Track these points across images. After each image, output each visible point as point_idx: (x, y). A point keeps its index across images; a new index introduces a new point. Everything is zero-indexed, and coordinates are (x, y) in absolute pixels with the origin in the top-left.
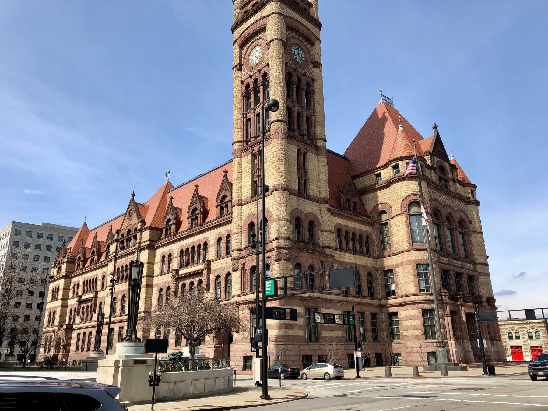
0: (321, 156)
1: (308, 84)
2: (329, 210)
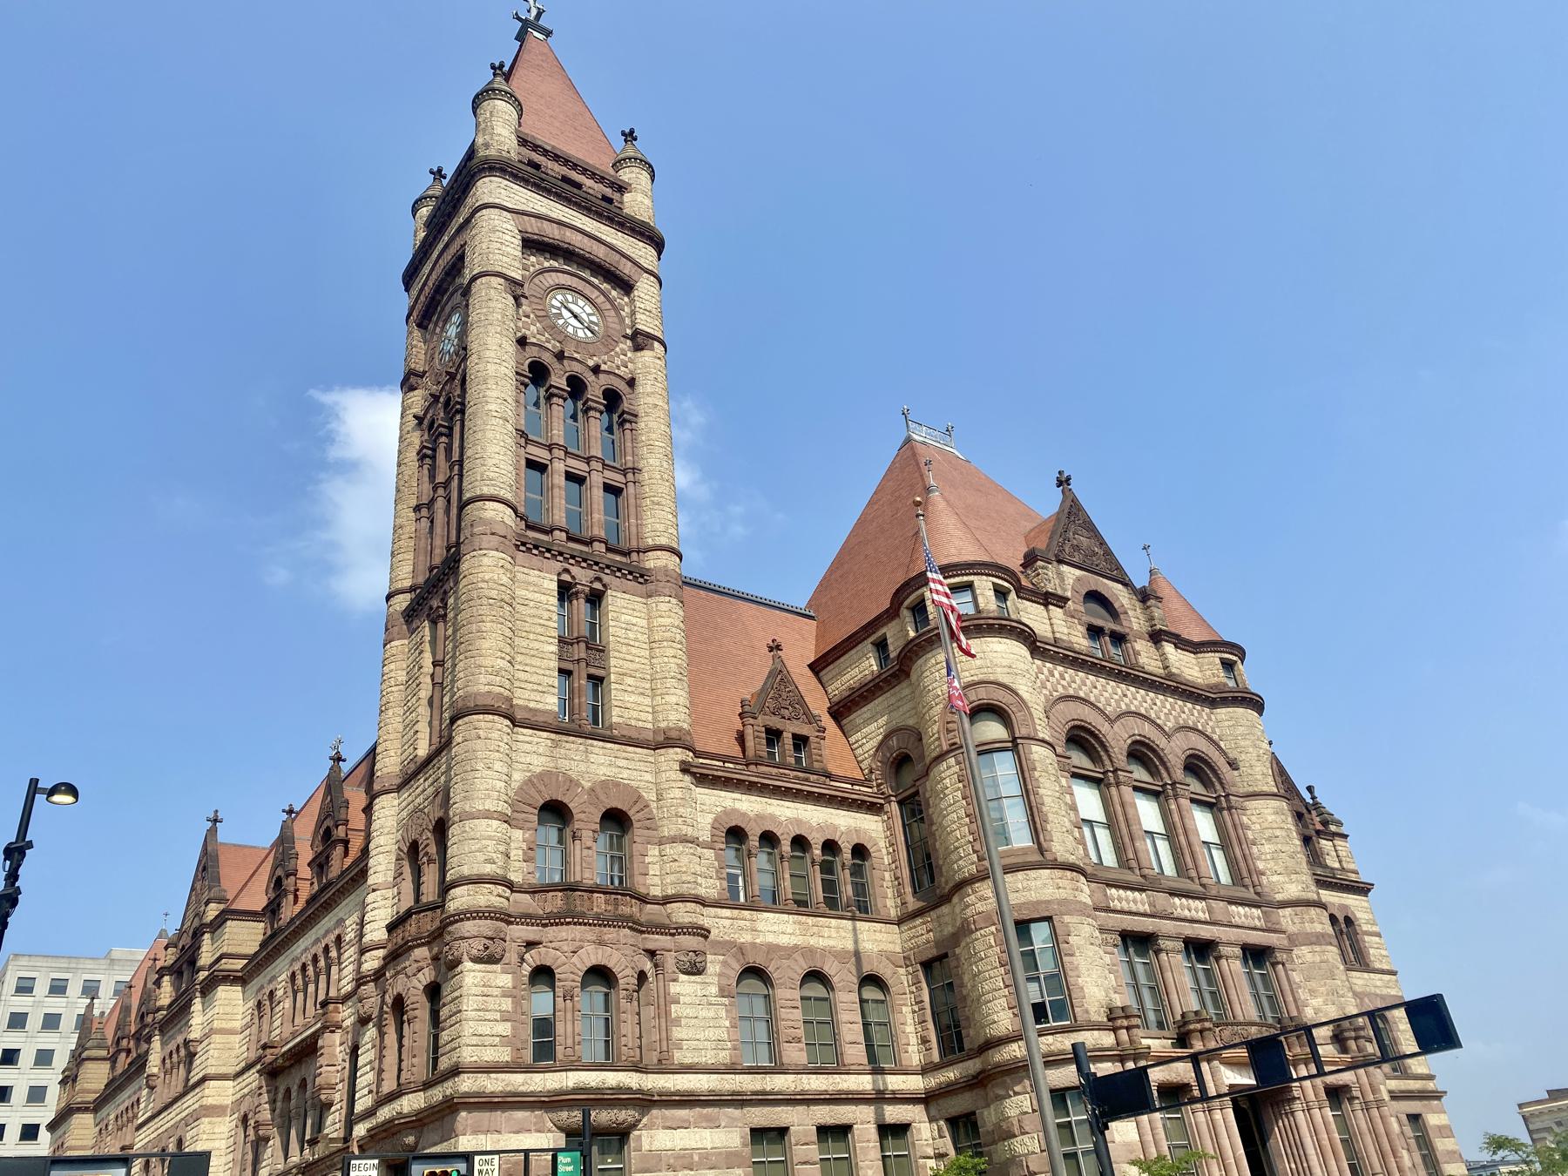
1: (612, 399)
2: (685, 769)
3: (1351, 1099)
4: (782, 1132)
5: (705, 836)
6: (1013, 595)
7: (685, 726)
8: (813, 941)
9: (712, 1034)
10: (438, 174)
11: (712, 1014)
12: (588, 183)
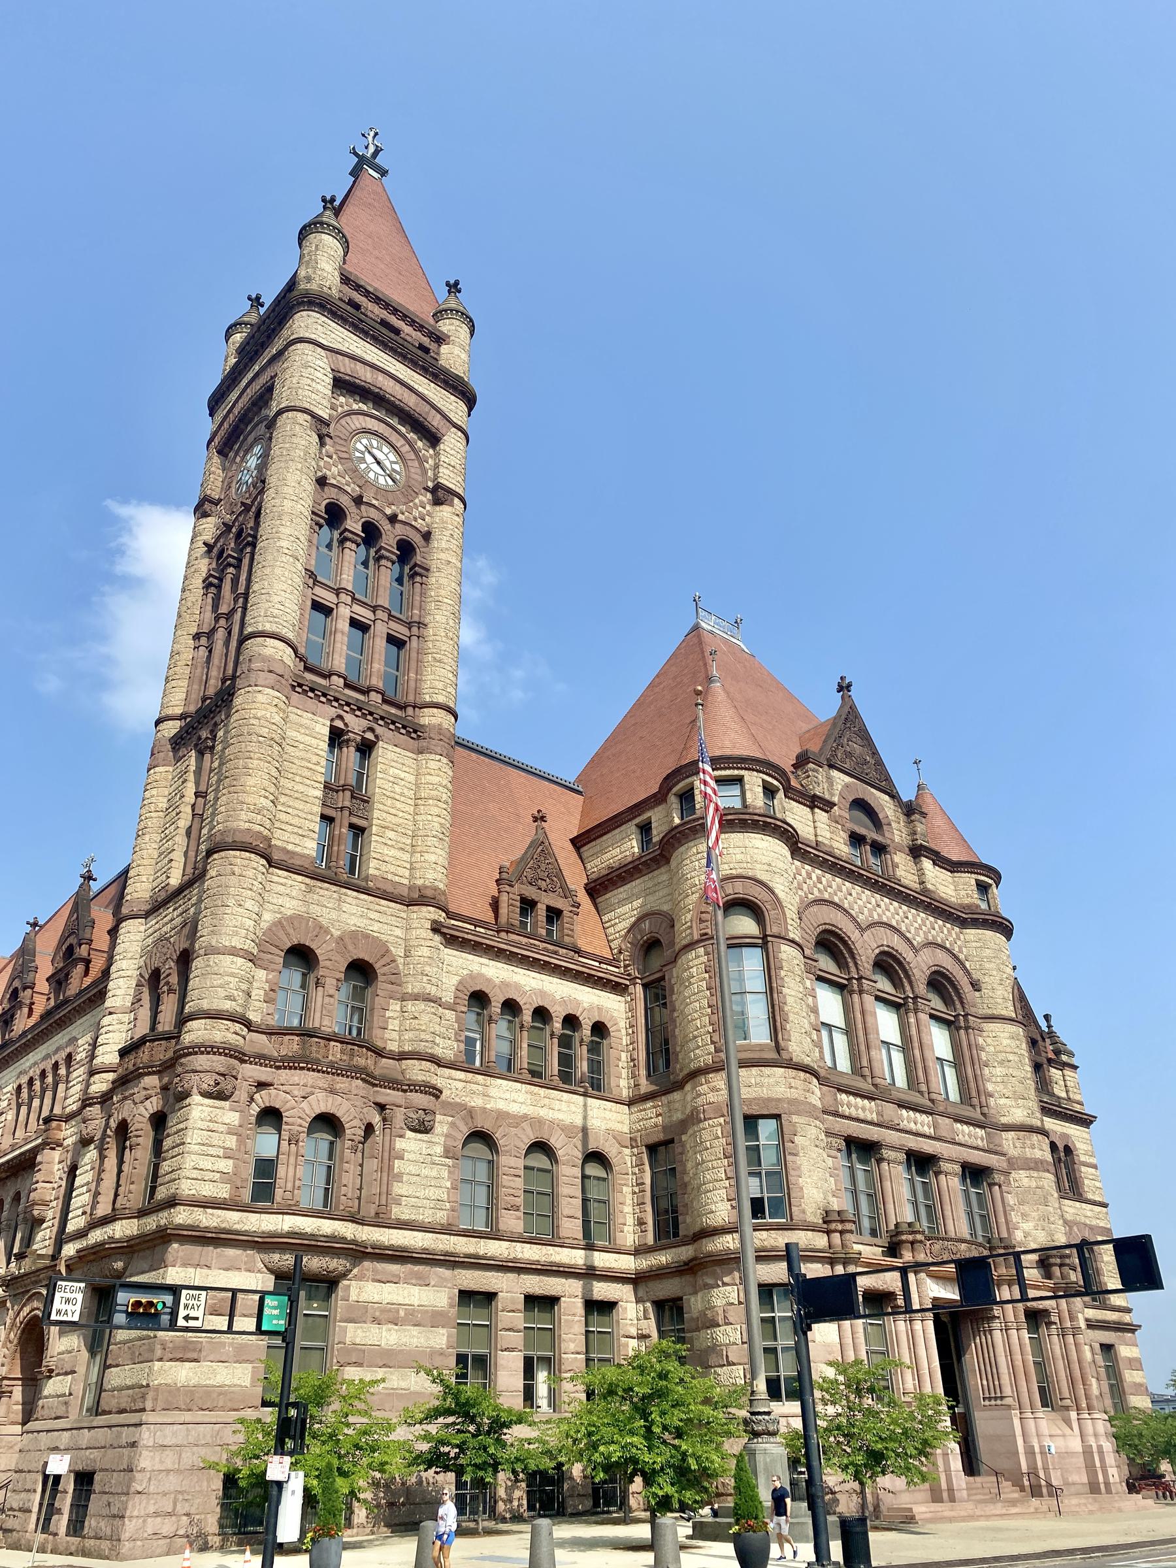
0: (433, 756)
1: (406, 550)
2: (436, 928)
3: (1049, 1324)
4: (489, 1297)
5: (448, 997)
6: (781, 794)
7: (441, 886)
8: (543, 1113)
9: (433, 1193)
10: (256, 301)
11: (434, 1173)
12: (407, 329)
